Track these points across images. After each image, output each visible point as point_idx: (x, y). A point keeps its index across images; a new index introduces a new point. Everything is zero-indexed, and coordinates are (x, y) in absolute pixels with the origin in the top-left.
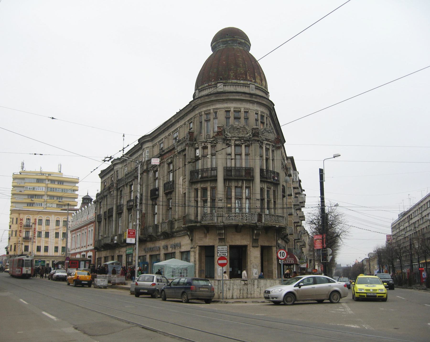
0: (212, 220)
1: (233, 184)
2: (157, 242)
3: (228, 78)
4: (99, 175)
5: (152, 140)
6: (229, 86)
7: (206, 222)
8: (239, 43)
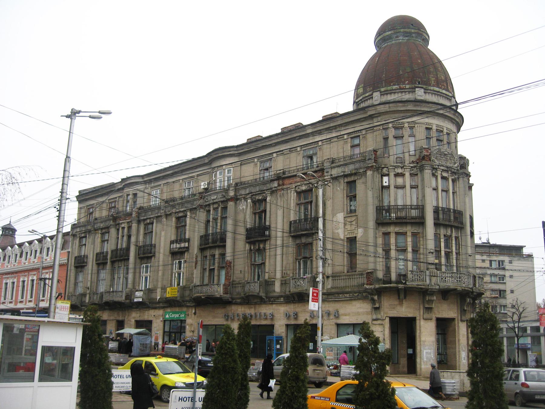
0: (423, 281)
1: (442, 231)
2: (264, 306)
3: (428, 83)
4: (77, 197)
5: (240, 155)
6: (430, 94)
7: (414, 283)
8: (423, 40)
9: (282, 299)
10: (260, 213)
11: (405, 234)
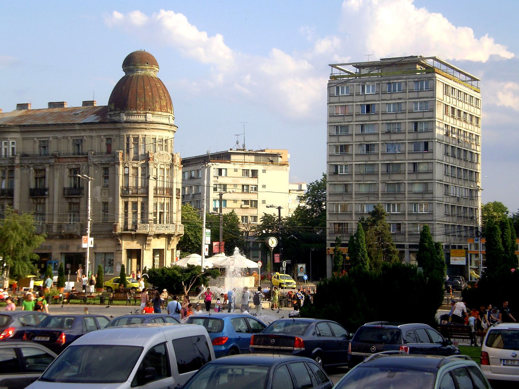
9: (58, 237)
10: (40, 177)
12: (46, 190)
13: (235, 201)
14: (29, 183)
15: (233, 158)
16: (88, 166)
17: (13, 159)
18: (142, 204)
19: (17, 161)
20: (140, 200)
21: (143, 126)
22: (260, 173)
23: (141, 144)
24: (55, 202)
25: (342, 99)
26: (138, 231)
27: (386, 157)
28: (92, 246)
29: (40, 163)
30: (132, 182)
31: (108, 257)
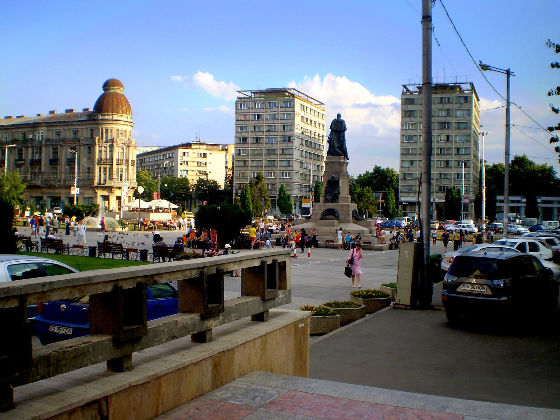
10: (55, 152)
11: (106, 168)
12: (58, 160)
13: (193, 171)
14: (49, 156)
15: (193, 146)
16: (80, 146)
17: (41, 142)
18: (110, 169)
19: (44, 143)
20: (108, 166)
21: (111, 122)
22: (208, 155)
23: (109, 134)
24: (63, 166)
25: (244, 111)
26: (106, 185)
27: (267, 145)
28: (78, 193)
29: (55, 145)
30: (103, 156)
31: (91, 200)
